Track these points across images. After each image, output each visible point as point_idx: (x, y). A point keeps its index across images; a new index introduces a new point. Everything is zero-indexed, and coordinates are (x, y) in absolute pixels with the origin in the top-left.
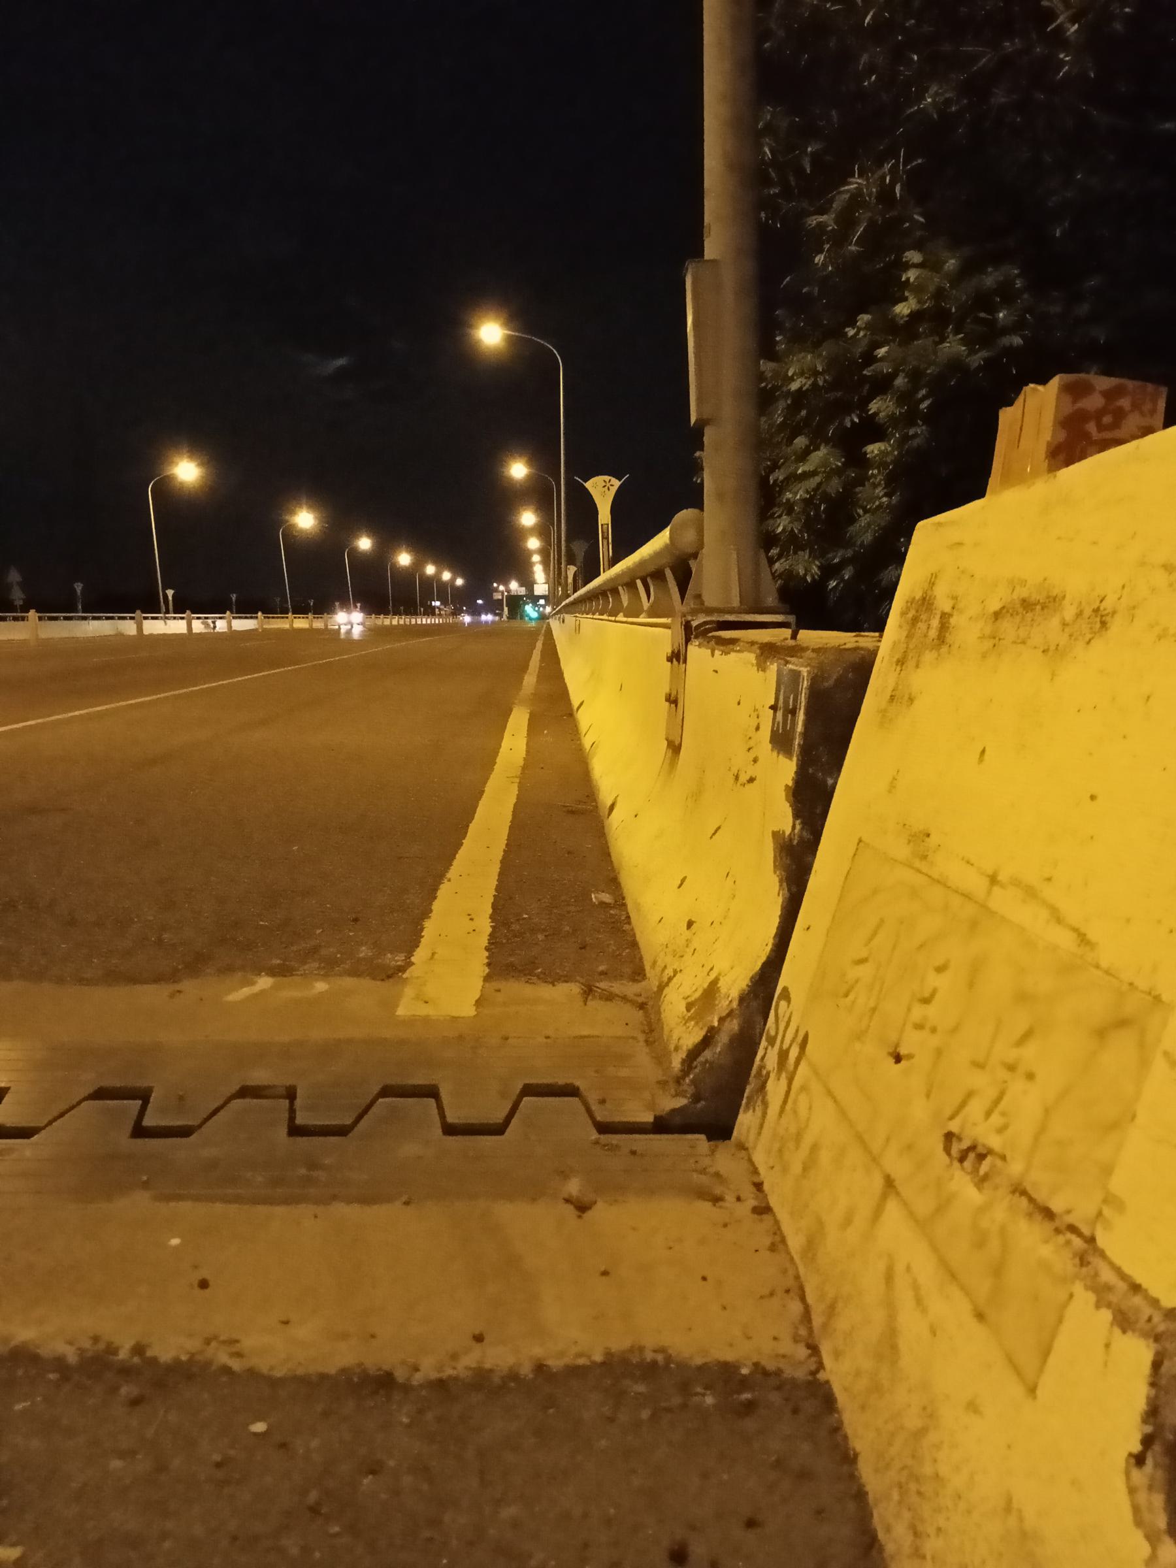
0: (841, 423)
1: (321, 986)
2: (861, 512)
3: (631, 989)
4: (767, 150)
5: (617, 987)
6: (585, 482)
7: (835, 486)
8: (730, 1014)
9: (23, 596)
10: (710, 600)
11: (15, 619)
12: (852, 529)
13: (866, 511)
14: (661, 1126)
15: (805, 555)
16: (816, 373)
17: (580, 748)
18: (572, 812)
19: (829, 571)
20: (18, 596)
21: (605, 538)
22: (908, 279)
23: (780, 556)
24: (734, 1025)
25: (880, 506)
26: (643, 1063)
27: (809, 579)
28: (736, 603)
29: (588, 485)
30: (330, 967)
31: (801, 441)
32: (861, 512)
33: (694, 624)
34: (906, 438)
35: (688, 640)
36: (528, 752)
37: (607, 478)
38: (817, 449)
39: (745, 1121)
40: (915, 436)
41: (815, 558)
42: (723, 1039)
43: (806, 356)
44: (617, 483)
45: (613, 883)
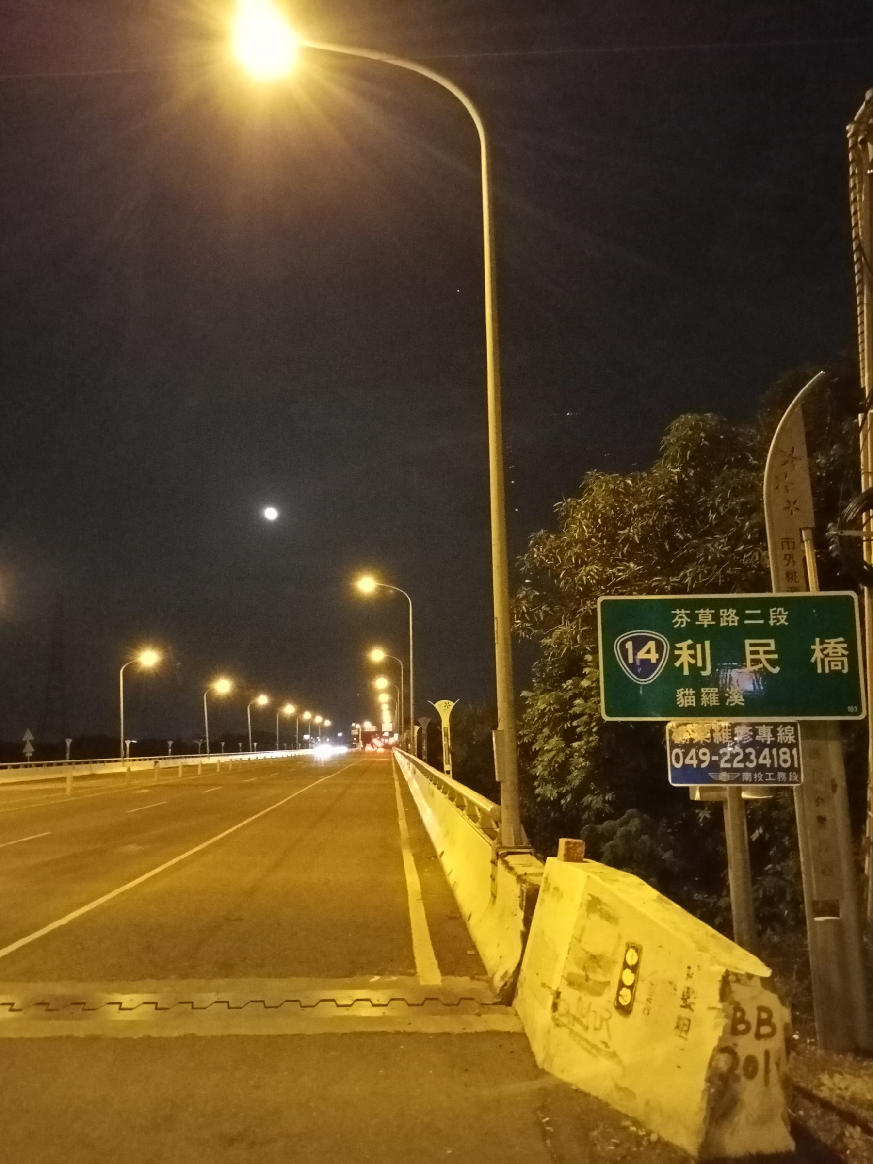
0: (563, 726)
1: (394, 978)
2: (573, 769)
3: (484, 978)
4: (524, 608)
5: (481, 977)
6: (434, 703)
7: (561, 758)
8: (511, 977)
9: (33, 750)
10: (505, 843)
11: (26, 766)
12: (570, 777)
13: (576, 769)
14: (494, 1004)
15: (550, 786)
16: (550, 704)
17: (446, 882)
18: (450, 918)
19: (561, 796)
20: (29, 750)
21: (446, 735)
22: (585, 672)
23: (539, 785)
24: (512, 980)
25: (582, 767)
26: (490, 994)
27: (552, 799)
28: (513, 845)
29: (436, 705)
30: (393, 973)
31: (546, 731)
32: (573, 769)
33: (500, 853)
34: (588, 742)
35: (497, 859)
36: (421, 883)
37: (447, 701)
38: (552, 737)
39: (515, 1002)
40: (592, 741)
41: (555, 788)
42: (509, 984)
43: (545, 696)
44: (452, 704)
45: (474, 947)
